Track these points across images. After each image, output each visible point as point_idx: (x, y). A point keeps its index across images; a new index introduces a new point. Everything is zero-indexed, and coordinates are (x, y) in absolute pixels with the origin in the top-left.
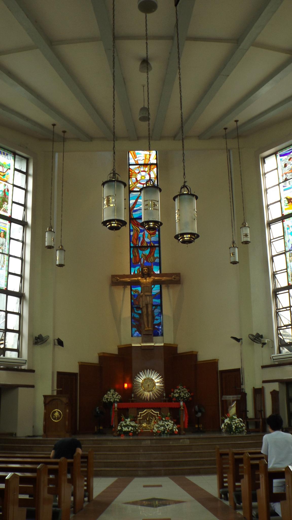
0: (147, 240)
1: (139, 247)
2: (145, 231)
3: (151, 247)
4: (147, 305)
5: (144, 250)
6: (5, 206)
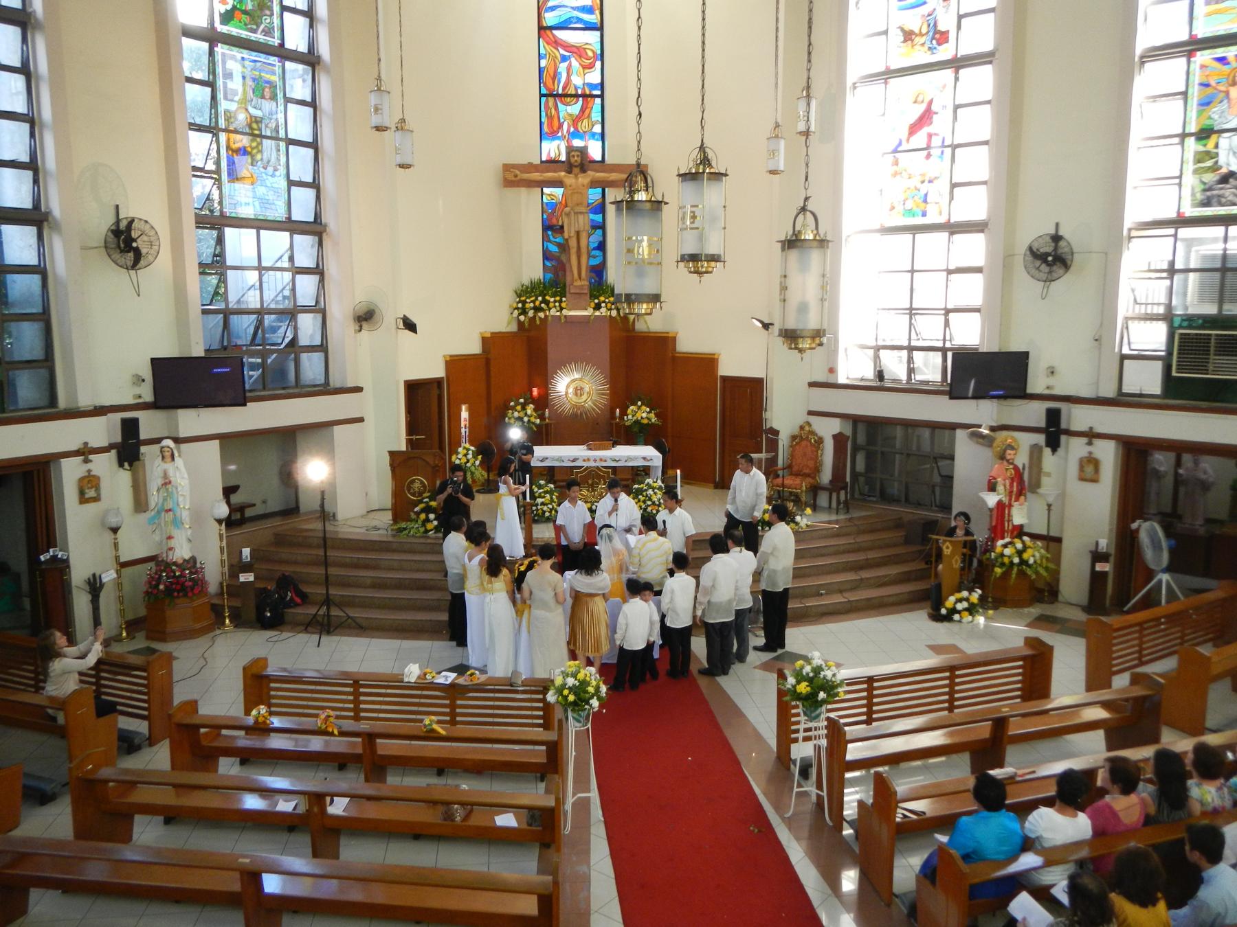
0: (577, 81)
1: (558, 95)
2: (573, 60)
3: (584, 96)
4: (578, 233)
6: (266, 21)
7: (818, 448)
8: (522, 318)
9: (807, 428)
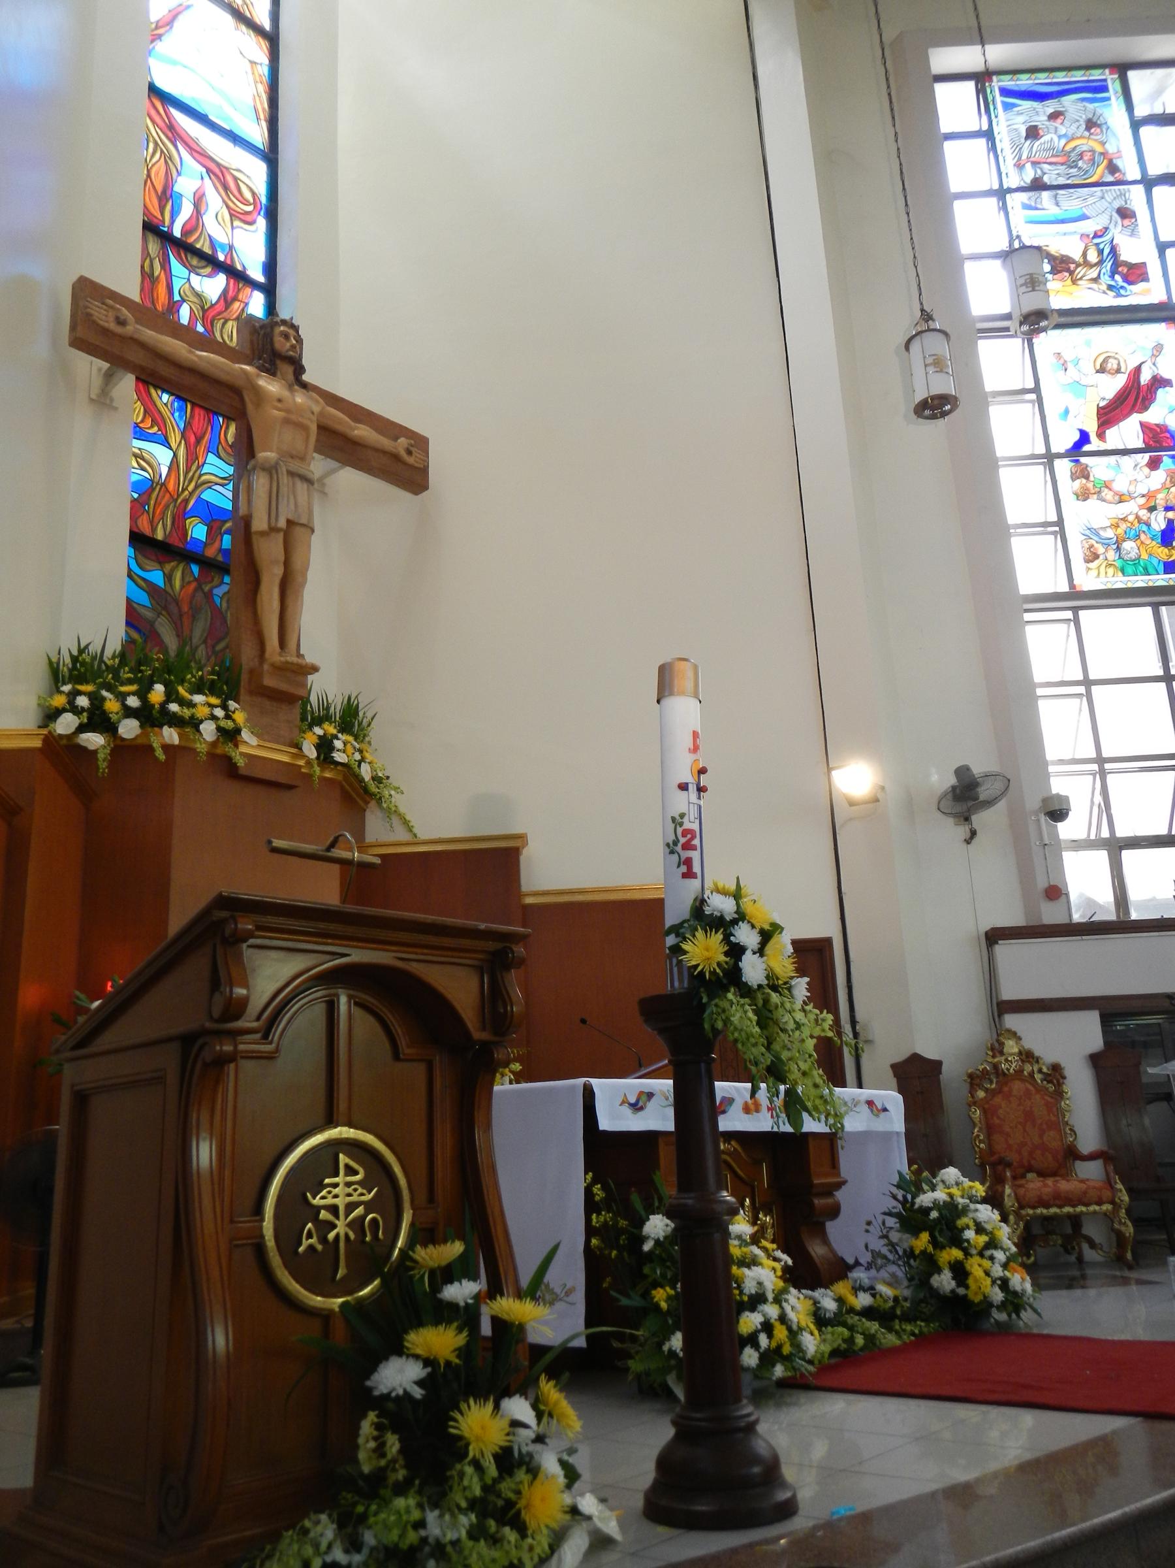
5: (192, 269)
7: (1059, 1094)
8: (94, 740)
9: (1011, 1047)
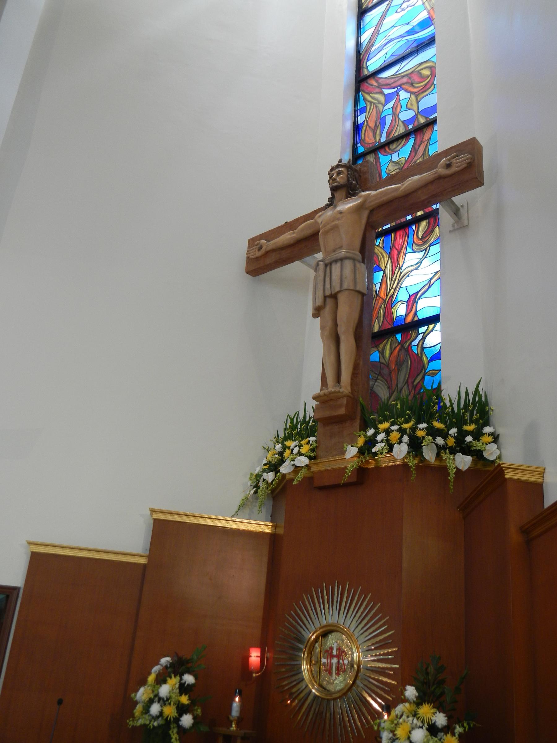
0: (406, 115)
